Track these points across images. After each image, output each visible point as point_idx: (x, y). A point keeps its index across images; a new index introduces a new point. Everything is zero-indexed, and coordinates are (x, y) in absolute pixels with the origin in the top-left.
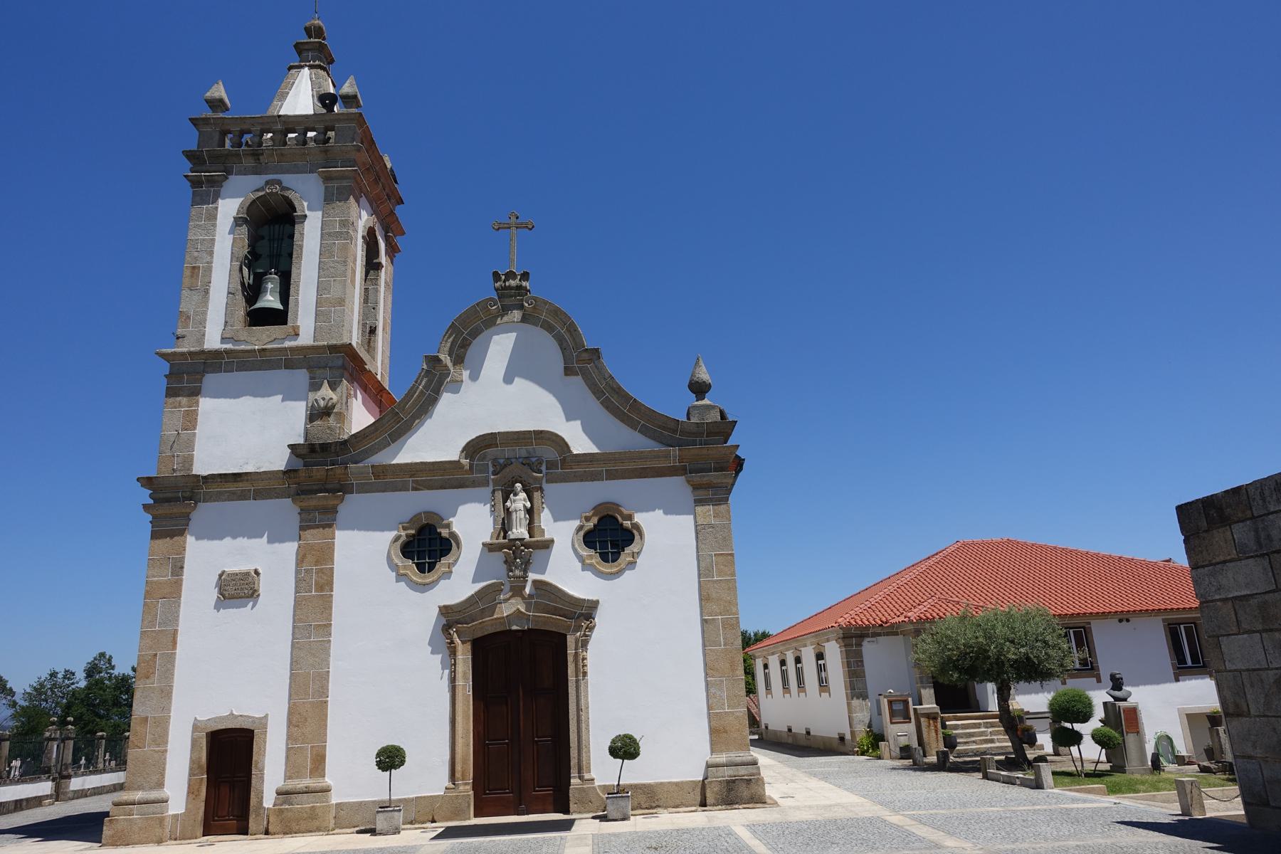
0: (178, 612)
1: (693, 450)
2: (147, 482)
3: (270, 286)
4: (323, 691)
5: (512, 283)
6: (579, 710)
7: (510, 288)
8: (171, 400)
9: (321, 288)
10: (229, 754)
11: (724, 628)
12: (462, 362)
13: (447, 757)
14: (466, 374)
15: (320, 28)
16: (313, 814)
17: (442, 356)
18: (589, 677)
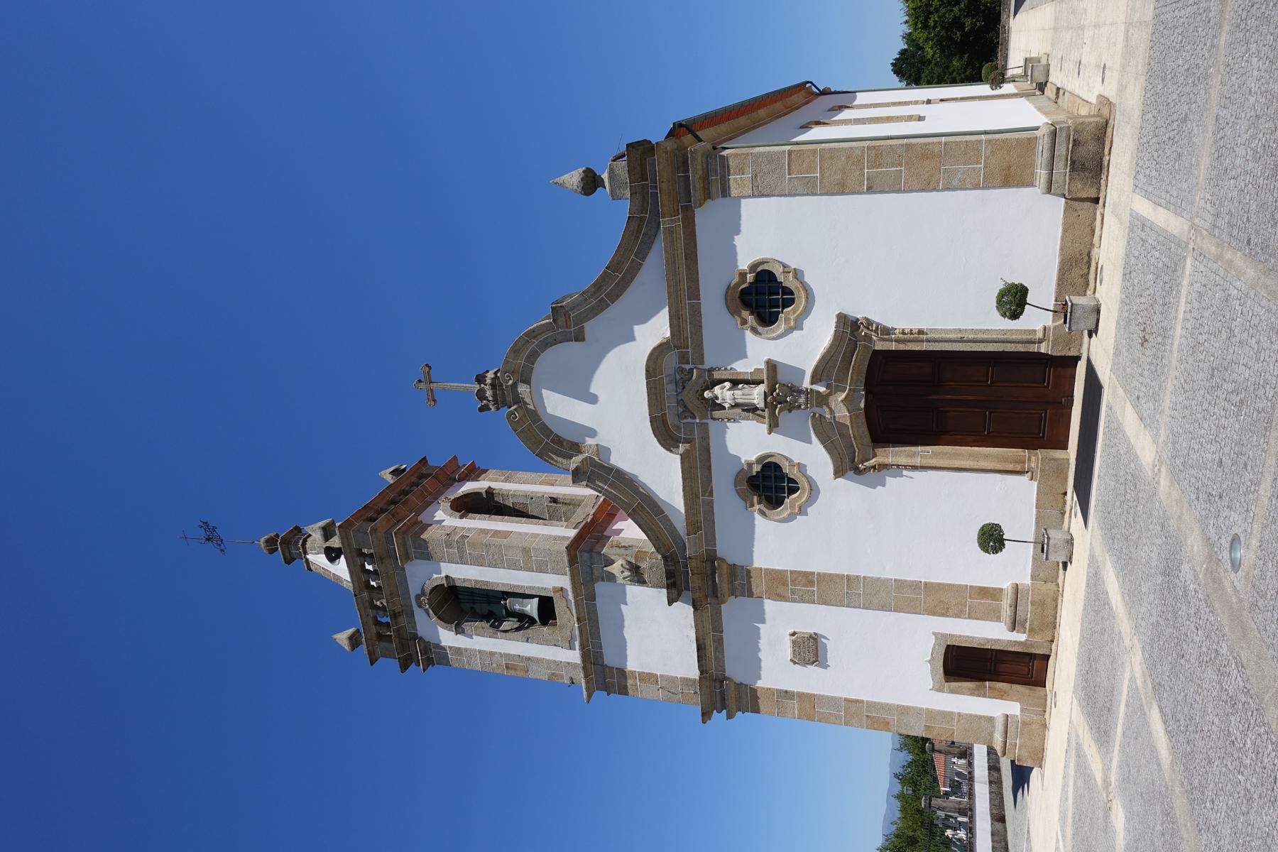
0: (828, 697)
1: (663, 199)
2: (706, 715)
3: (517, 607)
4: (915, 585)
5: (489, 393)
6: (961, 340)
7: (495, 395)
8: (630, 692)
9: (514, 566)
10: (964, 664)
11: (880, 166)
12: (577, 444)
13: (998, 476)
14: (590, 441)
15: (267, 541)
16: (1040, 604)
17: (573, 466)
18: (924, 327)
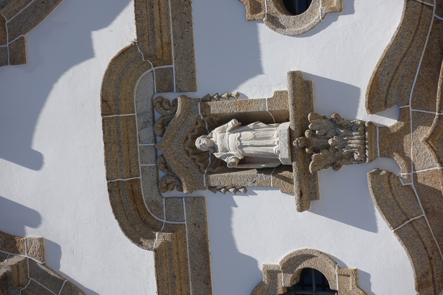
14: (31, 233)
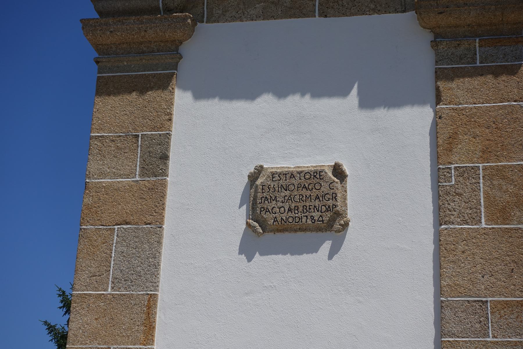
0: (156, 255)
